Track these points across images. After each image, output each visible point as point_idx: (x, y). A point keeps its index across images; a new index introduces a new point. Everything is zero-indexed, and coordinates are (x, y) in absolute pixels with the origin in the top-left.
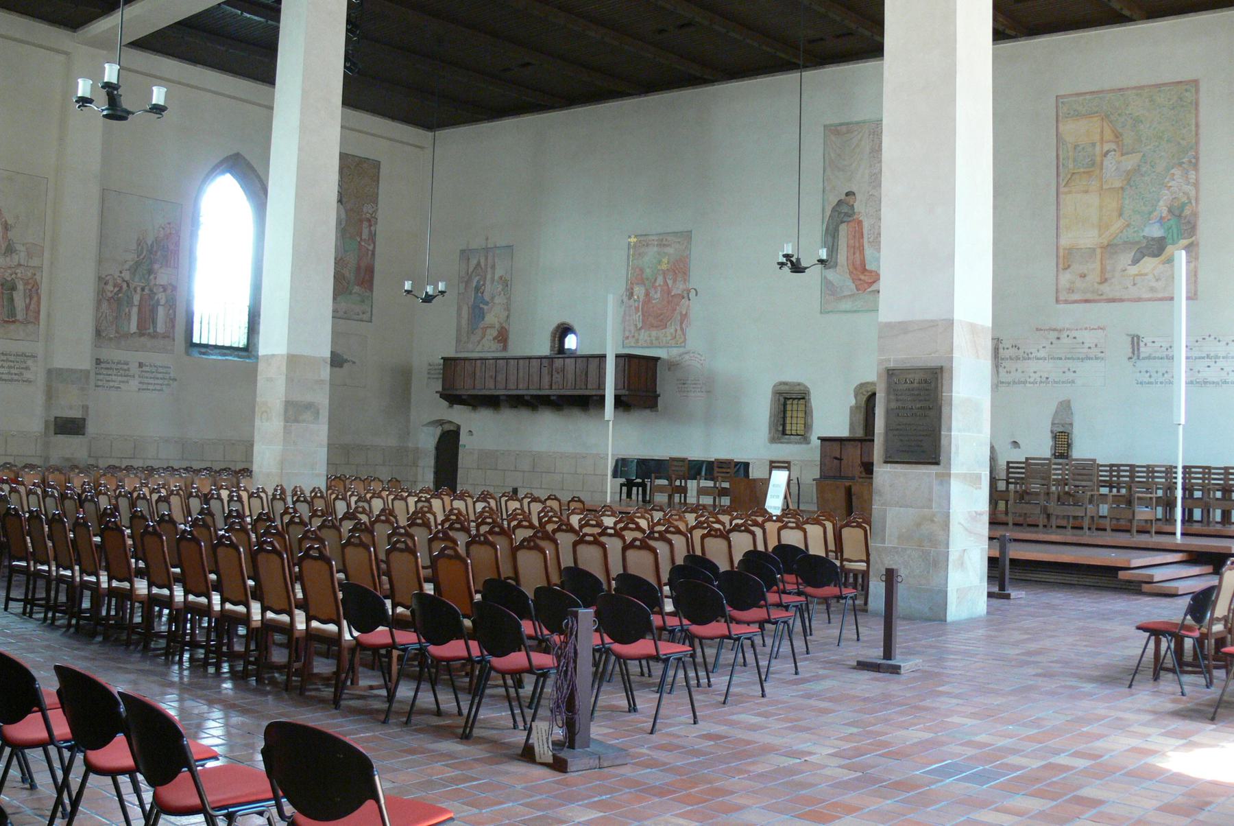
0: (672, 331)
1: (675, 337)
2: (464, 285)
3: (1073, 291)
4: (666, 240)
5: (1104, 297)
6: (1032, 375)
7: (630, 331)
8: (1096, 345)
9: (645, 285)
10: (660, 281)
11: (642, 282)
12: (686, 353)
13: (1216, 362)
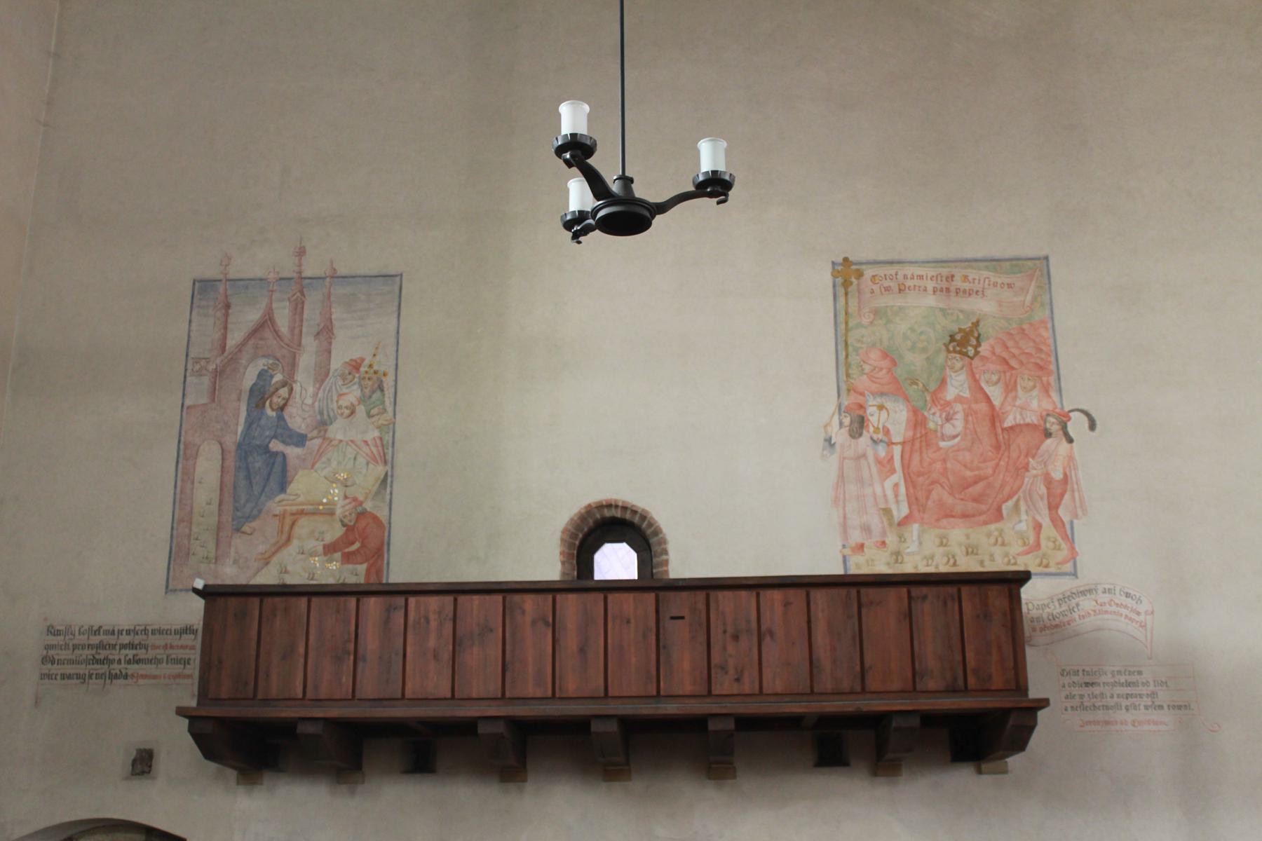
0: (1024, 526)
1: (1038, 545)
2: (206, 381)
4: (965, 278)
7: (866, 529)
9: (906, 399)
10: (957, 386)
11: (896, 389)
12: (1083, 593)
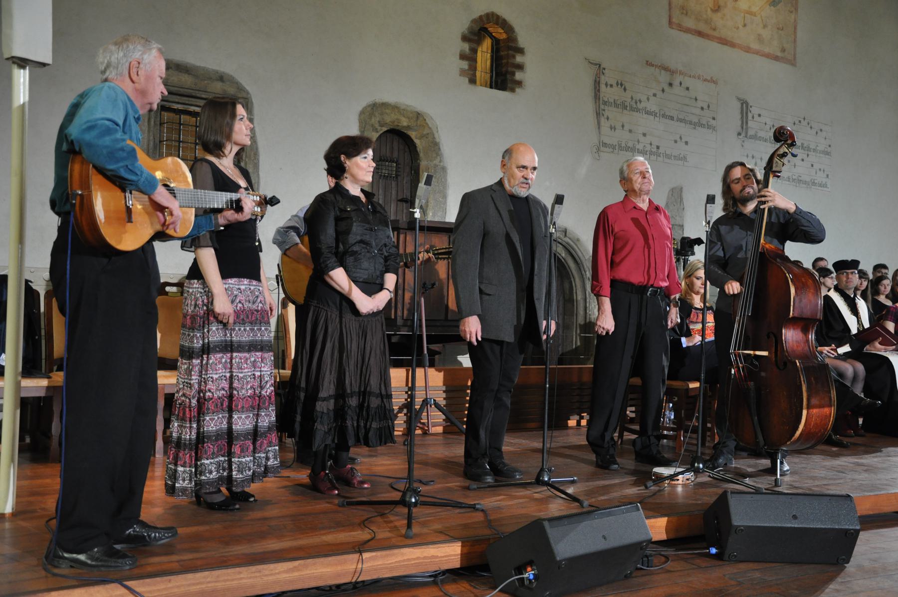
3: (687, 14)
5: (716, 34)
6: (642, 138)
8: (709, 106)
13: (808, 155)
